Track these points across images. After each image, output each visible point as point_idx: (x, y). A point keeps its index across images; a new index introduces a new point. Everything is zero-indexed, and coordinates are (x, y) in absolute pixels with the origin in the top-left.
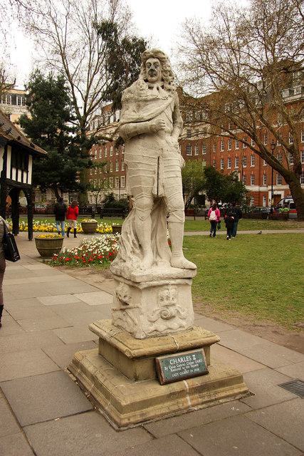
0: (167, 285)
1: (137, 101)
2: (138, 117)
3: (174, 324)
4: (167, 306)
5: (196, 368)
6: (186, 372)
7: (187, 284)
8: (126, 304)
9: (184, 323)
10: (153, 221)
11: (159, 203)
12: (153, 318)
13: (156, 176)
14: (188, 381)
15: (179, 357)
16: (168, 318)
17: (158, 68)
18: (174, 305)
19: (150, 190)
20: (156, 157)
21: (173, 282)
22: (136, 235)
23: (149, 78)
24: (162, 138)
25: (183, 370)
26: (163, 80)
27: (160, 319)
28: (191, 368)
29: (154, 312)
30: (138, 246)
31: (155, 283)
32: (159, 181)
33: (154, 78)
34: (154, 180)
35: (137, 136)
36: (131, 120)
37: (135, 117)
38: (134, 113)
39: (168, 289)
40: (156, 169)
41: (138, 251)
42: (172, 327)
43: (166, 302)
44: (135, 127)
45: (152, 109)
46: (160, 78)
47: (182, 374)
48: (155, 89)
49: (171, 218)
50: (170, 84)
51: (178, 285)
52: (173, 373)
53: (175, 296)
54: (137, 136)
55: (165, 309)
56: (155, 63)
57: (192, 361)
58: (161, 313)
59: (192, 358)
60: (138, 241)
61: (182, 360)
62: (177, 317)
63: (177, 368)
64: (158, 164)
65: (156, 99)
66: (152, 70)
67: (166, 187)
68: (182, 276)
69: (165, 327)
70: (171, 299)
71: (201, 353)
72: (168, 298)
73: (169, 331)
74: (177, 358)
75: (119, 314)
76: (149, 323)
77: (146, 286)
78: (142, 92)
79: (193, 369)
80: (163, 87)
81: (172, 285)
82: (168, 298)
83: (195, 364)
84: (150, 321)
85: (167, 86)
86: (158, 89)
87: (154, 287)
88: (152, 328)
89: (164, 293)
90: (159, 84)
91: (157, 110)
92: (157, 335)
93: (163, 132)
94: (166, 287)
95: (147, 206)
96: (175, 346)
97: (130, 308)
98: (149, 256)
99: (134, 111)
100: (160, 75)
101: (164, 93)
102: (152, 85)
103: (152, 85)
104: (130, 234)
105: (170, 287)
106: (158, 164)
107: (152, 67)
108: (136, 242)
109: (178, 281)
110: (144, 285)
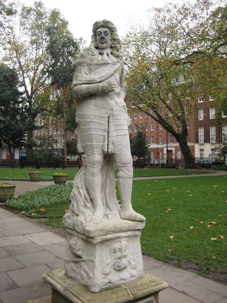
0: (119, 237)
1: (88, 65)
2: (90, 79)
3: (125, 275)
4: (120, 258)
7: (137, 236)
8: (79, 257)
9: (134, 272)
10: (103, 176)
11: (109, 159)
12: (108, 270)
13: (106, 134)
17: (108, 36)
19: (101, 147)
20: (107, 116)
22: (87, 190)
23: (100, 45)
24: (112, 99)
26: (111, 47)
27: (113, 271)
29: (107, 265)
30: (89, 200)
31: (109, 236)
32: (110, 139)
33: (104, 45)
34: (104, 138)
35: (91, 95)
36: (84, 82)
37: (87, 79)
38: (85, 76)
39: (120, 242)
40: (107, 128)
41: (89, 205)
43: (119, 254)
44: (88, 88)
45: (105, 71)
46: (110, 45)
48: (105, 55)
49: (120, 174)
50: (118, 51)
51: (129, 237)
53: (127, 247)
54: (91, 95)
55: (118, 260)
56: (105, 32)
58: (114, 265)
60: (89, 195)
62: (128, 268)
64: (108, 122)
65: (106, 64)
66: (102, 38)
67: (116, 144)
68: (132, 228)
69: (118, 279)
72: (120, 250)
73: (122, 282)
75: (73, 266)
76: (103, 276)
77: (100, 240)
78: (93, 57)
80: (112, 53)
81: (124, 237)
82: (120, 250)
86: (108, 55)
87: (107, 240)
88: (106, 281)
89: (117, 245)
90: (109, 51)
91: (108, 73)
93: (112, 93)
94: (119, 240)
95: (98, 162)
96: (129, 298)
97: (84, 261)
98: (101, 210)
99: (86, 74)
100: (110, 43)
101: (113, 59)
102: (102, 51)
103: (102, 51)
104: (82, 189)
105: (122, 240)
106: (108, 122)
107: (103, 35)
108: (87, 196)
109: (129, 233)
110: (98, 239)
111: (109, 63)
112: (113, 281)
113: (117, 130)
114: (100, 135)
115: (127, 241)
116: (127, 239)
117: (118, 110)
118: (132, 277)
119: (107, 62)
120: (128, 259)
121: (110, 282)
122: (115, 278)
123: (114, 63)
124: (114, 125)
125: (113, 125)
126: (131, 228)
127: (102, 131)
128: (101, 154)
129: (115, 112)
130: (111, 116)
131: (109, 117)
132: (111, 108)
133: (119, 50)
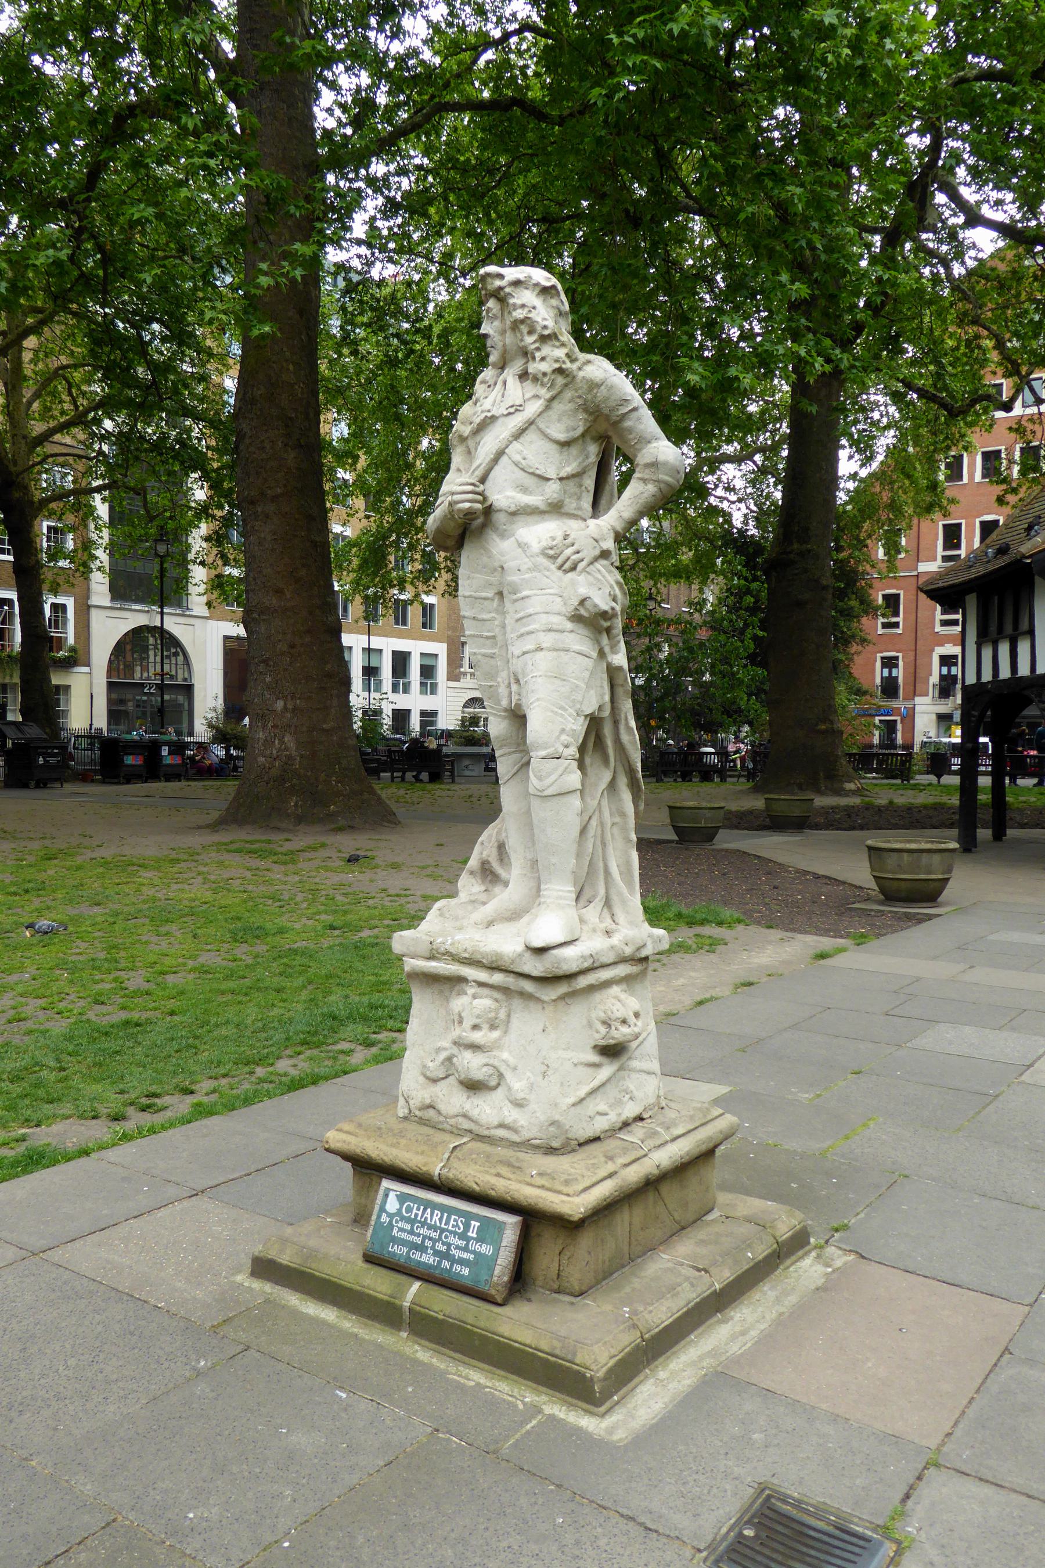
5: (462, 1262)
6: (428, 1258)
14: (425, 1285)
15: (434, 1206)
16: (473, 1086)
18: (475, 1047)
21: (483, 976)
24: (503, 536)
25: (421, 1248)
28: (446, 1255)
42: (474, 1113)
47: (416, 1256)
51: (505, 990)
52: (395, 1240)
57: (463, 1236)
59: (467, 1226)
61: (436, 1218)
62: (499, 1094)
63: (411, 1232)
70: (467, 1024)
71: (501, 1226)
74: (427, 1204)
76: (421, 1079)
79: (453, 1260)
81: (481, 984)
83: (466, 1249)
84: (428, 1078)
85: (534, 367)
92: (426, 1119)
109: (498, 978)
111: (493, 419)
112: (441, 1107)
113: (522, 635)
114: (484, 655)
115: (496, 1000)
116: (497, 995)
117: (524, 568)
118: (501, 1126)
119: (489, 415)
120: (496, 1063)
121: (431, 1106)
122: (453, 1101)
123: (512, 410)
124: (517, 620)
125: (513, 621)
126: (505, 963)
127: (488, 642)
128: (505, 718)
129: (513, 578)
130: (505, 593)
131: (500, 594)
132: (497, 564)
133: (538, 355)
